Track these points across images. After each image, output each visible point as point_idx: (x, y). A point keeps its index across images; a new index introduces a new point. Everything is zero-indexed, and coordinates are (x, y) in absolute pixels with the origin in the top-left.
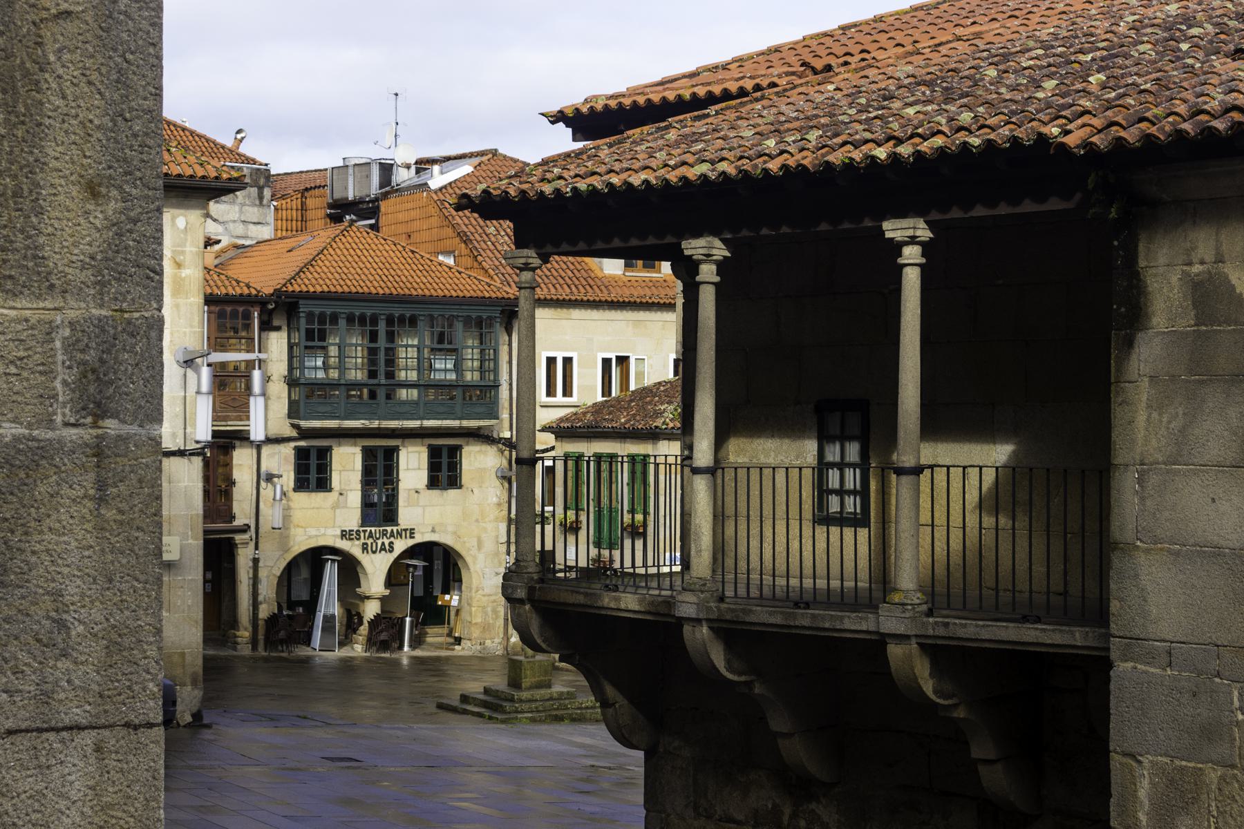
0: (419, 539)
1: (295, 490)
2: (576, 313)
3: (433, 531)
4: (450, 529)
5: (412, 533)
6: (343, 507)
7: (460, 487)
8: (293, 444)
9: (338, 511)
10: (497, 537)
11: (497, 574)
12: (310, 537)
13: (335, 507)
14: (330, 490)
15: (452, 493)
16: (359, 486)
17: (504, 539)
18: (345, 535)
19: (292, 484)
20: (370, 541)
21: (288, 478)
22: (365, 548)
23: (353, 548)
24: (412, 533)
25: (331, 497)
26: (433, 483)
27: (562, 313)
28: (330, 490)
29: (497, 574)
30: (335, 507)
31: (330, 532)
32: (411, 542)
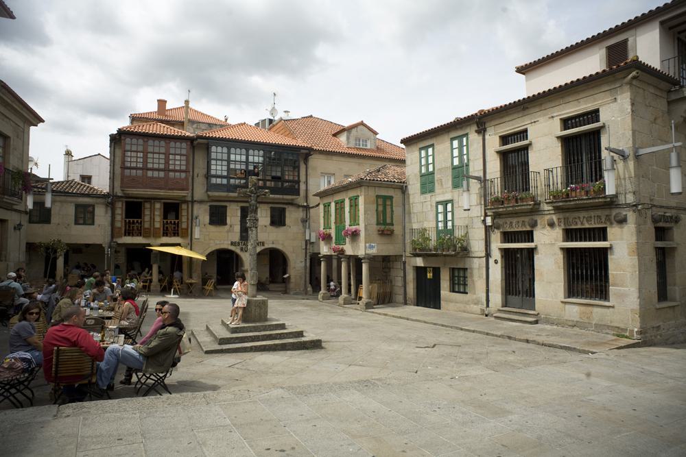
0: (266, 246)
1: (210, 224)
2: (335, 158)
3: (273, 243)
4: (281, 242)
5: (263, 245)
6: (233, 232)
7: (284, 225)
8: (209, 204)
9: (230, 234)
10: (302, 246)
11: (302, 262)
12: (216, 244)
13: (228, 231)
14: (225, 224)
15: (283, 228)
16: (239, 223)
17: (304, 247)
18: (232, 244)
19: (208, 222)
20: (244, 247)
21: (206, 218)
22: (242, 249)
23: (237, 250)
24: (263, 244)
25: (227, 227)
26: (273, 223)
27: (329, 157)
28: (226, 224)
29: (302, 262)
30: (228, 231)
31: (225, 242)
32: (263, 248)
